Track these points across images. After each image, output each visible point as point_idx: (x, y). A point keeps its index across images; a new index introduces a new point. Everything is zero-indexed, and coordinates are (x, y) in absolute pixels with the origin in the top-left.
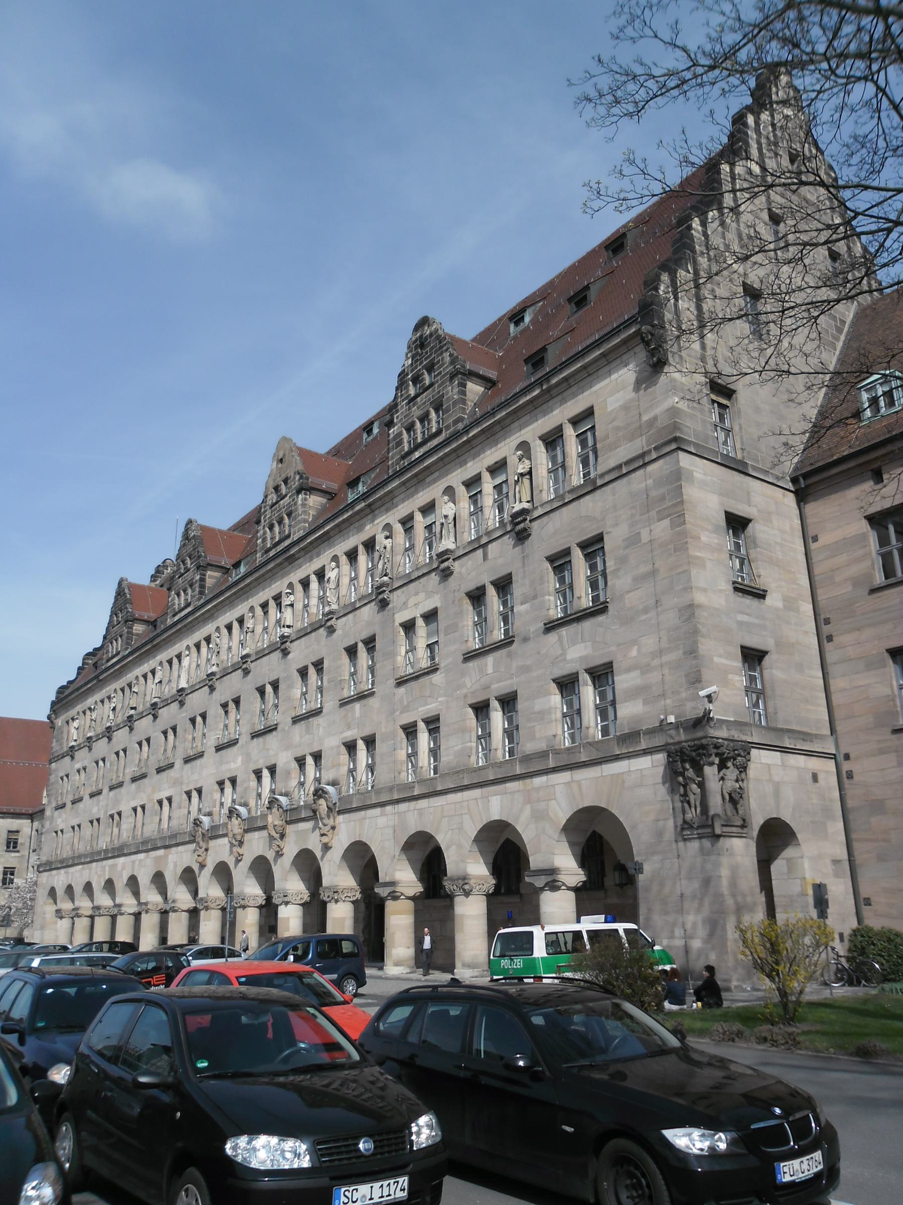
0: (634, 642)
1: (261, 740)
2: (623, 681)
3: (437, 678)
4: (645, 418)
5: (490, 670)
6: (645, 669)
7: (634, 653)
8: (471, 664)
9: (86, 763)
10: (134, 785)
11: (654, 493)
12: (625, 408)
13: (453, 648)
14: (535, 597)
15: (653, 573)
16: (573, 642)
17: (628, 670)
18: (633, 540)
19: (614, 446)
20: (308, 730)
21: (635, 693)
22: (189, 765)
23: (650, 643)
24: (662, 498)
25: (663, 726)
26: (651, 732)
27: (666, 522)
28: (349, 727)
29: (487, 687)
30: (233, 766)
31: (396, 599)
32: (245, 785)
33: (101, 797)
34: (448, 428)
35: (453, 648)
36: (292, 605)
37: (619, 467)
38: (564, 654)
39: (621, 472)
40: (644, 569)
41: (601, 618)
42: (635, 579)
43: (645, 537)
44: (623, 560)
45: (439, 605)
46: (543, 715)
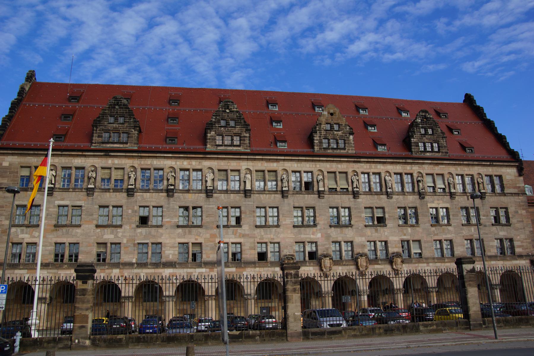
0: (519, 235)
1: (338, 230)
2: (516, 243)
3: (450, 228)
4: (517, 185)
5: (473, 231)
6: (522, 242)
7: (519, 237)
8: (465, 227)
9: (78, 203)
10: (180, 230)
11: (521, 204)
12: (511, 180)
13: (457, 221)
14: (487, 216)
15: (523, 221)
16: (501, 231)
17: (517, 241)
18: (516, 212)
19: (509, 188)
20: (376, 231)
21: (519, 247)
22: (262, 230)
23: (523, 236)
24: (523, 205)
25: (527, 256)
26: (526, 256)
27: (525, 211)
28: (405, 235)
29: (472, 235)
30: (312, 236)
31: (427, 198)
32: (327, 246)
33: (119, 230)
34: (442, 152)
35: (457, 221)
36: (358, 180)
37: (512, 194)
38: (498, 232)
39: (512, 194)
40: (519, 220)
41: (509, 227)
42: (518, 221)
43: (519, 212)
44: (514, 216)
45: (449, 207)
46: (492, 246)
